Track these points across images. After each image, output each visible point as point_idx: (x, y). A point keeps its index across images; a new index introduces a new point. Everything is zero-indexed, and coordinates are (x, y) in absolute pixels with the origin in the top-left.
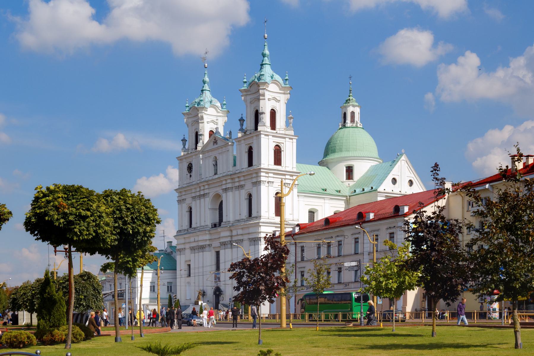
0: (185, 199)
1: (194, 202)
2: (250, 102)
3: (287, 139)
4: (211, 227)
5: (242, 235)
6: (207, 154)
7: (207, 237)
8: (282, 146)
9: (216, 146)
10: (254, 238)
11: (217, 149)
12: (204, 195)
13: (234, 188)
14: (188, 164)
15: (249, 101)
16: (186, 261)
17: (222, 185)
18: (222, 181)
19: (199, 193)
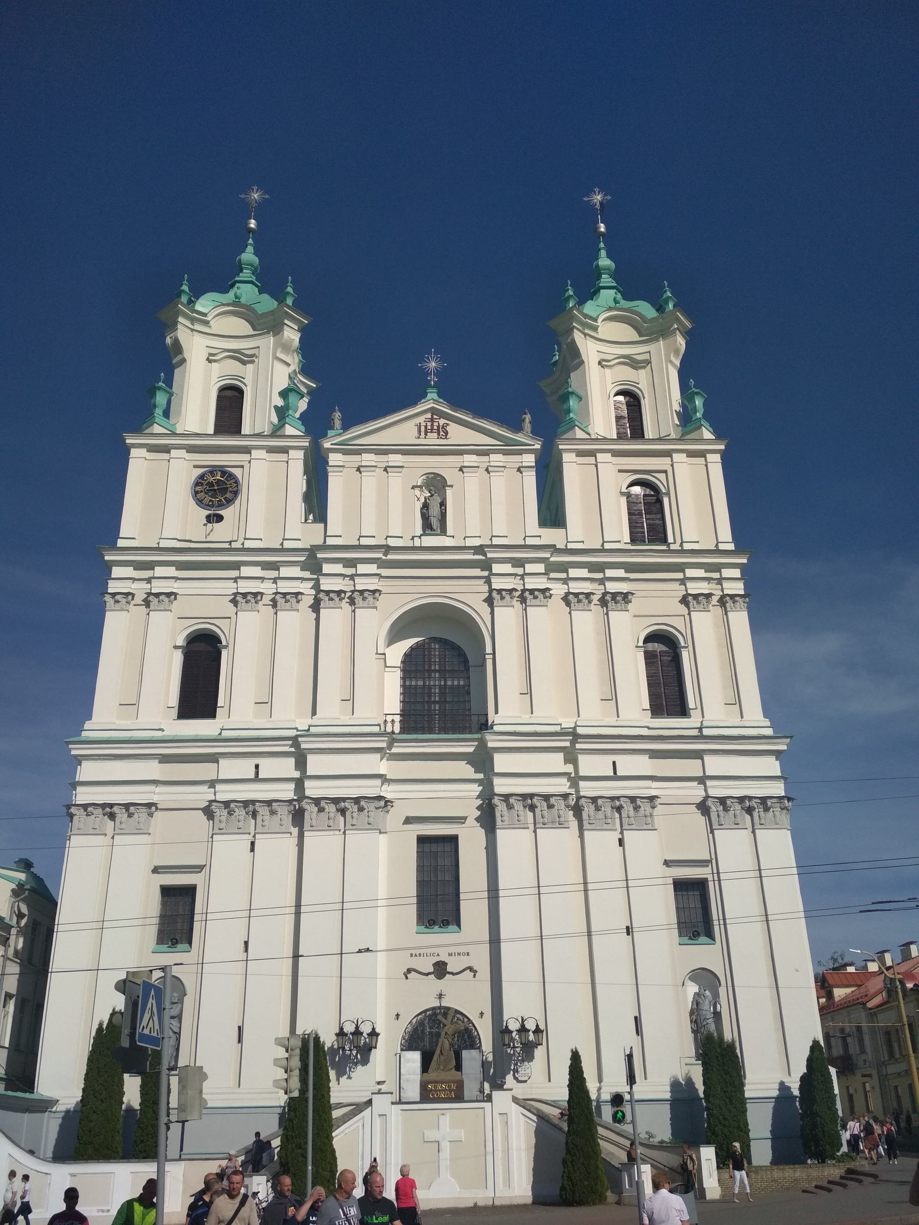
0: (175, 594)
2: (600, 363)
9: (432, 439)
10: (750, 798)
14: (201, 471)
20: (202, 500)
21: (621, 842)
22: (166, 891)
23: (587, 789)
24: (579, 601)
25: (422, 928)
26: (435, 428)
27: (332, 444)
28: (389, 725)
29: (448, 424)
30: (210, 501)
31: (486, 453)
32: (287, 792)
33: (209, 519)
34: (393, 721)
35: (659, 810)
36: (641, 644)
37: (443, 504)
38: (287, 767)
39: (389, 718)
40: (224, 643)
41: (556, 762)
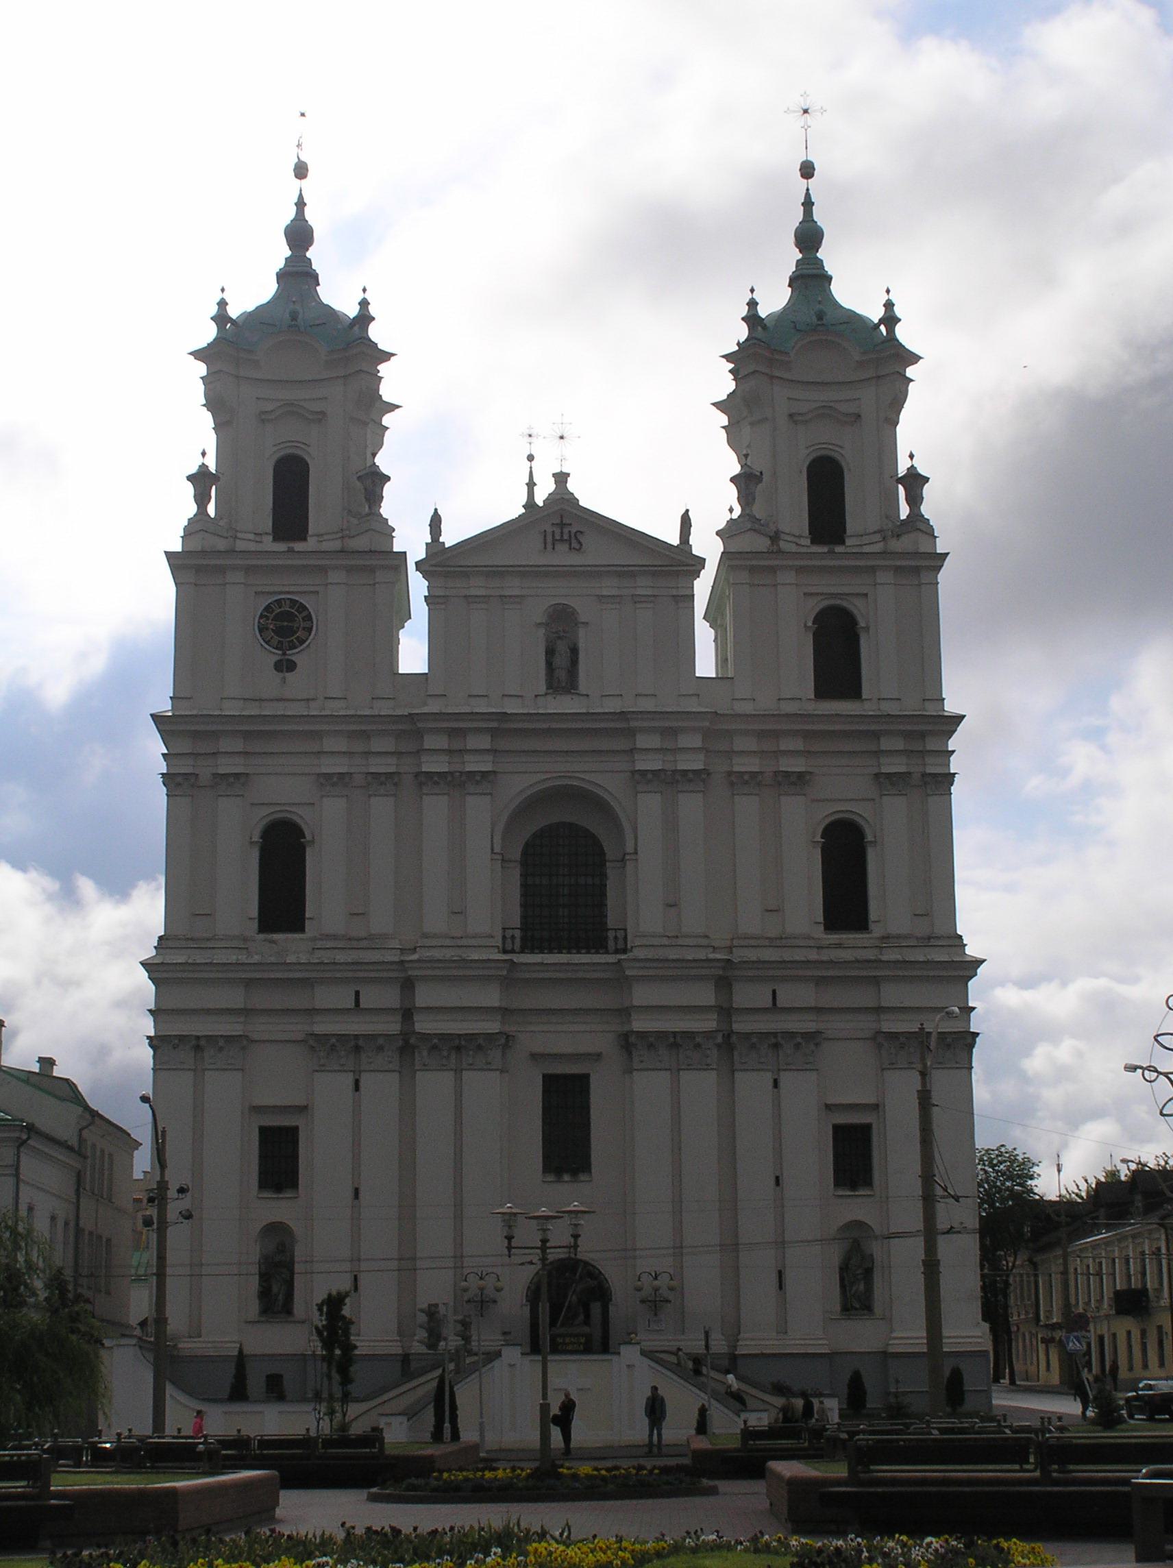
5: (819, 1010)
7: (491, 997)
9: (563, 557)
16: (257, 1110)
17: (631, 750)
18: (631, 733)
19: (393, 760)
20: (269, 641)
21: (776, 1084)
22: (265, 1132)
23: (741, 1025)
24: (746, 783)
25: (551, 1178)
26: (566, 537)
27: (432, 566)
28: (509, 941)
29: (581, 532)
30: (279, 642)
31: (632, 575)
32: (393, 1026)
33: (279, 666)
34: (513, 937)
36: (818, 838)
37: (574, 651)
38: (390, 997)
39: (509, 933)
40: (308, 837)
41: (705, 995)
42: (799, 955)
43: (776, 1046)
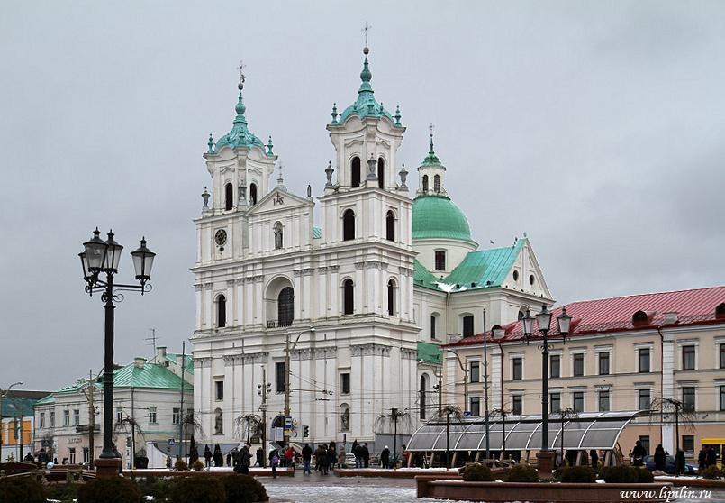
1: (230, 290)
3: (402, 204)
4: (266, 326)
6: (259, 217)
7: (259, 342)
8: (394, 212)
9: (279, 206)
11: (285, 210)
12: (253, 279)
13: (317, 270)
15: (342, 144)
35: (339, 350)
37: (281, 235)
42: (330, 323)
43: (325, 351)
